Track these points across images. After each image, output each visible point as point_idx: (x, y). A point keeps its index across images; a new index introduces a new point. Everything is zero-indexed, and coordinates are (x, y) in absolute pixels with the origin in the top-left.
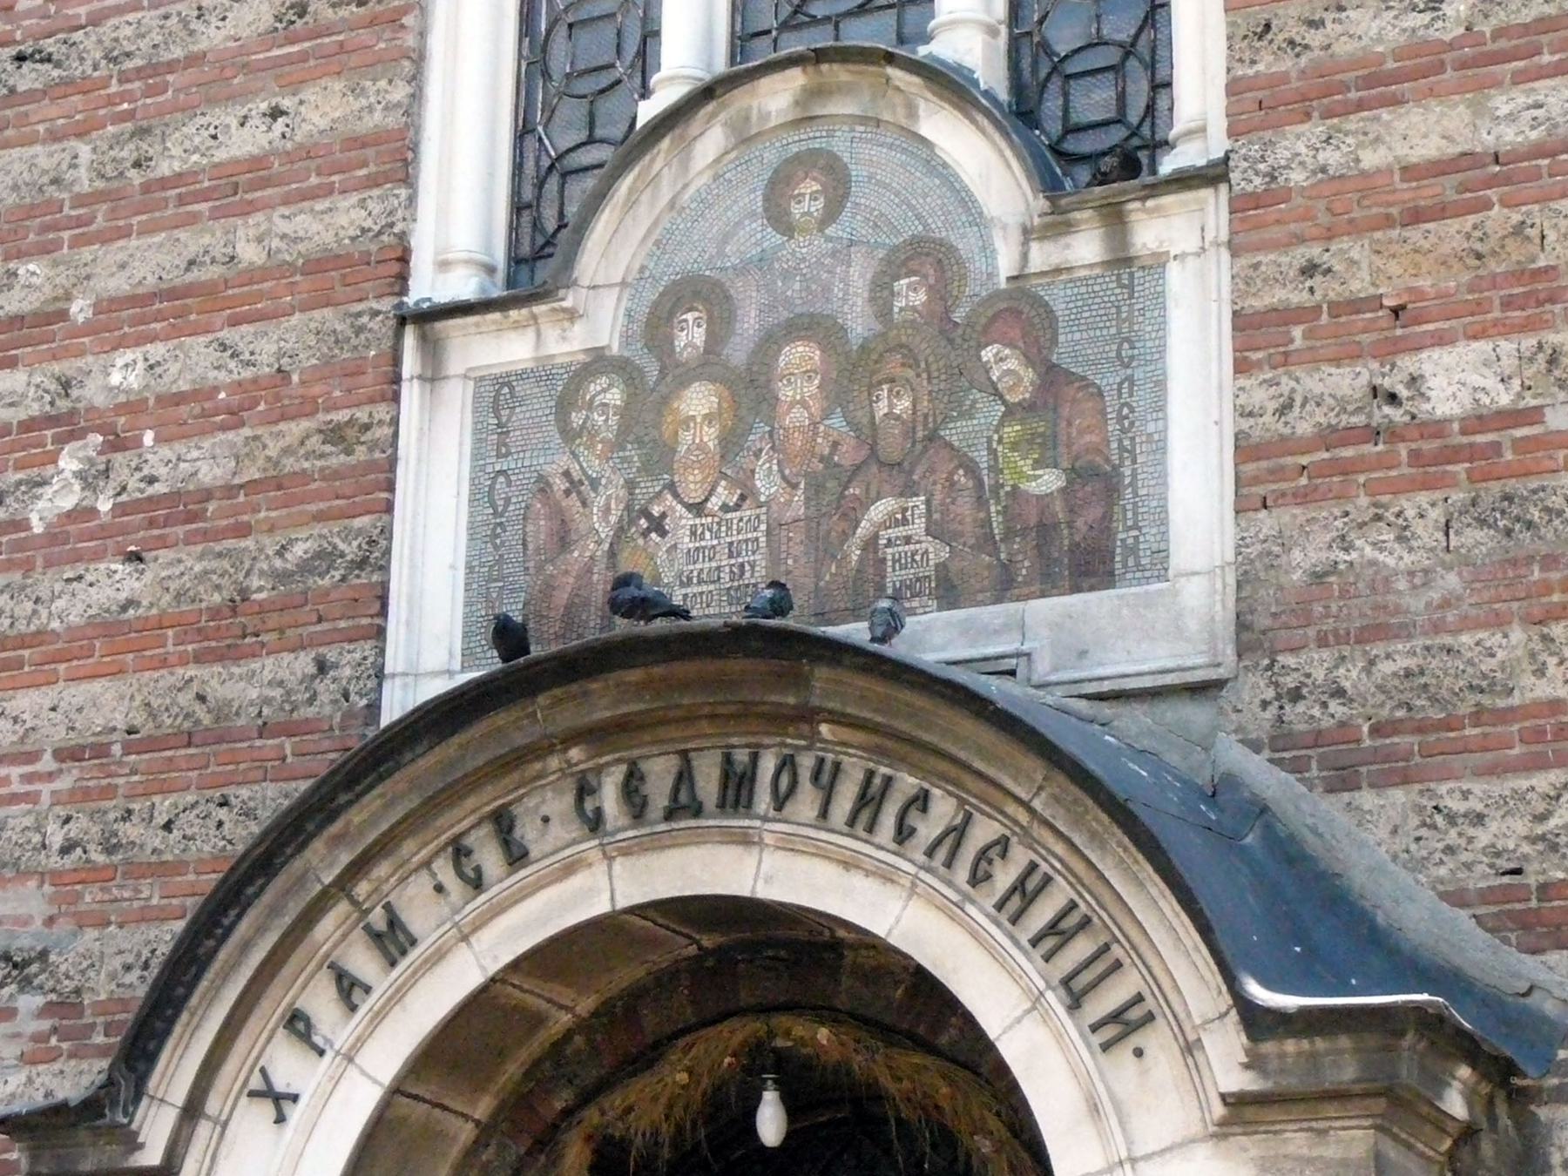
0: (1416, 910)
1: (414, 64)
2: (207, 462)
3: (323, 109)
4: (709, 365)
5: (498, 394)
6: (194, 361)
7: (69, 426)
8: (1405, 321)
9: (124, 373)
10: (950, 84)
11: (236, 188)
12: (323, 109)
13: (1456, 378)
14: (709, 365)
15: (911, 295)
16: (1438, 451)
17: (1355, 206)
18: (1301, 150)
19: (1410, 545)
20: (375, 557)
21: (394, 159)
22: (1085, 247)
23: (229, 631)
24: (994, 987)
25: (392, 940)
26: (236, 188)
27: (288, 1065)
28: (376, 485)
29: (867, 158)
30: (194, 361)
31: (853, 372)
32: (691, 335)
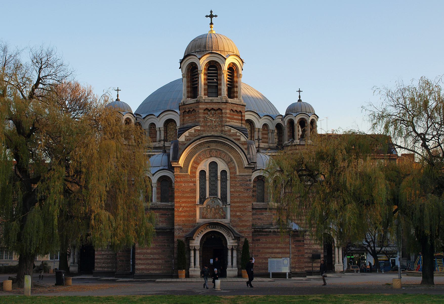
0: (236, 232)
1: (195, 193)
2: (188, 209)
3: (192, 195)
4: (209, 208)
5: (200, 208)
6: (186, 205)
7: (181, 207)
8: (236, 211)
9: (183, 205)
10: (219, 199)
11: (188, 197)
12: (192, 195)
13: (238, 214)
14: (209, 208)
15: (218, 207)
16: (238, 216)
17: (235, 207)
18: (233, 204)
19: (236, 219)
20: (196, 214)
21: (195, 197)
22: (225, 206)
23: (189, 216)
24: (225, 235)
25: (202, 231)
26: (188, 197)
27: (198, 235)
28: (196, 211)
29: (216, 201)
30: (186, 205)
31: (215, 209)
32: (208, 207)
